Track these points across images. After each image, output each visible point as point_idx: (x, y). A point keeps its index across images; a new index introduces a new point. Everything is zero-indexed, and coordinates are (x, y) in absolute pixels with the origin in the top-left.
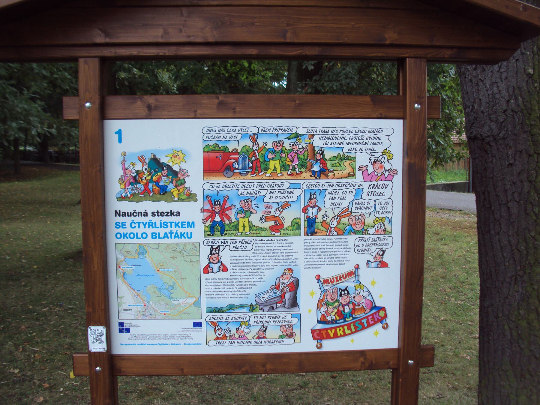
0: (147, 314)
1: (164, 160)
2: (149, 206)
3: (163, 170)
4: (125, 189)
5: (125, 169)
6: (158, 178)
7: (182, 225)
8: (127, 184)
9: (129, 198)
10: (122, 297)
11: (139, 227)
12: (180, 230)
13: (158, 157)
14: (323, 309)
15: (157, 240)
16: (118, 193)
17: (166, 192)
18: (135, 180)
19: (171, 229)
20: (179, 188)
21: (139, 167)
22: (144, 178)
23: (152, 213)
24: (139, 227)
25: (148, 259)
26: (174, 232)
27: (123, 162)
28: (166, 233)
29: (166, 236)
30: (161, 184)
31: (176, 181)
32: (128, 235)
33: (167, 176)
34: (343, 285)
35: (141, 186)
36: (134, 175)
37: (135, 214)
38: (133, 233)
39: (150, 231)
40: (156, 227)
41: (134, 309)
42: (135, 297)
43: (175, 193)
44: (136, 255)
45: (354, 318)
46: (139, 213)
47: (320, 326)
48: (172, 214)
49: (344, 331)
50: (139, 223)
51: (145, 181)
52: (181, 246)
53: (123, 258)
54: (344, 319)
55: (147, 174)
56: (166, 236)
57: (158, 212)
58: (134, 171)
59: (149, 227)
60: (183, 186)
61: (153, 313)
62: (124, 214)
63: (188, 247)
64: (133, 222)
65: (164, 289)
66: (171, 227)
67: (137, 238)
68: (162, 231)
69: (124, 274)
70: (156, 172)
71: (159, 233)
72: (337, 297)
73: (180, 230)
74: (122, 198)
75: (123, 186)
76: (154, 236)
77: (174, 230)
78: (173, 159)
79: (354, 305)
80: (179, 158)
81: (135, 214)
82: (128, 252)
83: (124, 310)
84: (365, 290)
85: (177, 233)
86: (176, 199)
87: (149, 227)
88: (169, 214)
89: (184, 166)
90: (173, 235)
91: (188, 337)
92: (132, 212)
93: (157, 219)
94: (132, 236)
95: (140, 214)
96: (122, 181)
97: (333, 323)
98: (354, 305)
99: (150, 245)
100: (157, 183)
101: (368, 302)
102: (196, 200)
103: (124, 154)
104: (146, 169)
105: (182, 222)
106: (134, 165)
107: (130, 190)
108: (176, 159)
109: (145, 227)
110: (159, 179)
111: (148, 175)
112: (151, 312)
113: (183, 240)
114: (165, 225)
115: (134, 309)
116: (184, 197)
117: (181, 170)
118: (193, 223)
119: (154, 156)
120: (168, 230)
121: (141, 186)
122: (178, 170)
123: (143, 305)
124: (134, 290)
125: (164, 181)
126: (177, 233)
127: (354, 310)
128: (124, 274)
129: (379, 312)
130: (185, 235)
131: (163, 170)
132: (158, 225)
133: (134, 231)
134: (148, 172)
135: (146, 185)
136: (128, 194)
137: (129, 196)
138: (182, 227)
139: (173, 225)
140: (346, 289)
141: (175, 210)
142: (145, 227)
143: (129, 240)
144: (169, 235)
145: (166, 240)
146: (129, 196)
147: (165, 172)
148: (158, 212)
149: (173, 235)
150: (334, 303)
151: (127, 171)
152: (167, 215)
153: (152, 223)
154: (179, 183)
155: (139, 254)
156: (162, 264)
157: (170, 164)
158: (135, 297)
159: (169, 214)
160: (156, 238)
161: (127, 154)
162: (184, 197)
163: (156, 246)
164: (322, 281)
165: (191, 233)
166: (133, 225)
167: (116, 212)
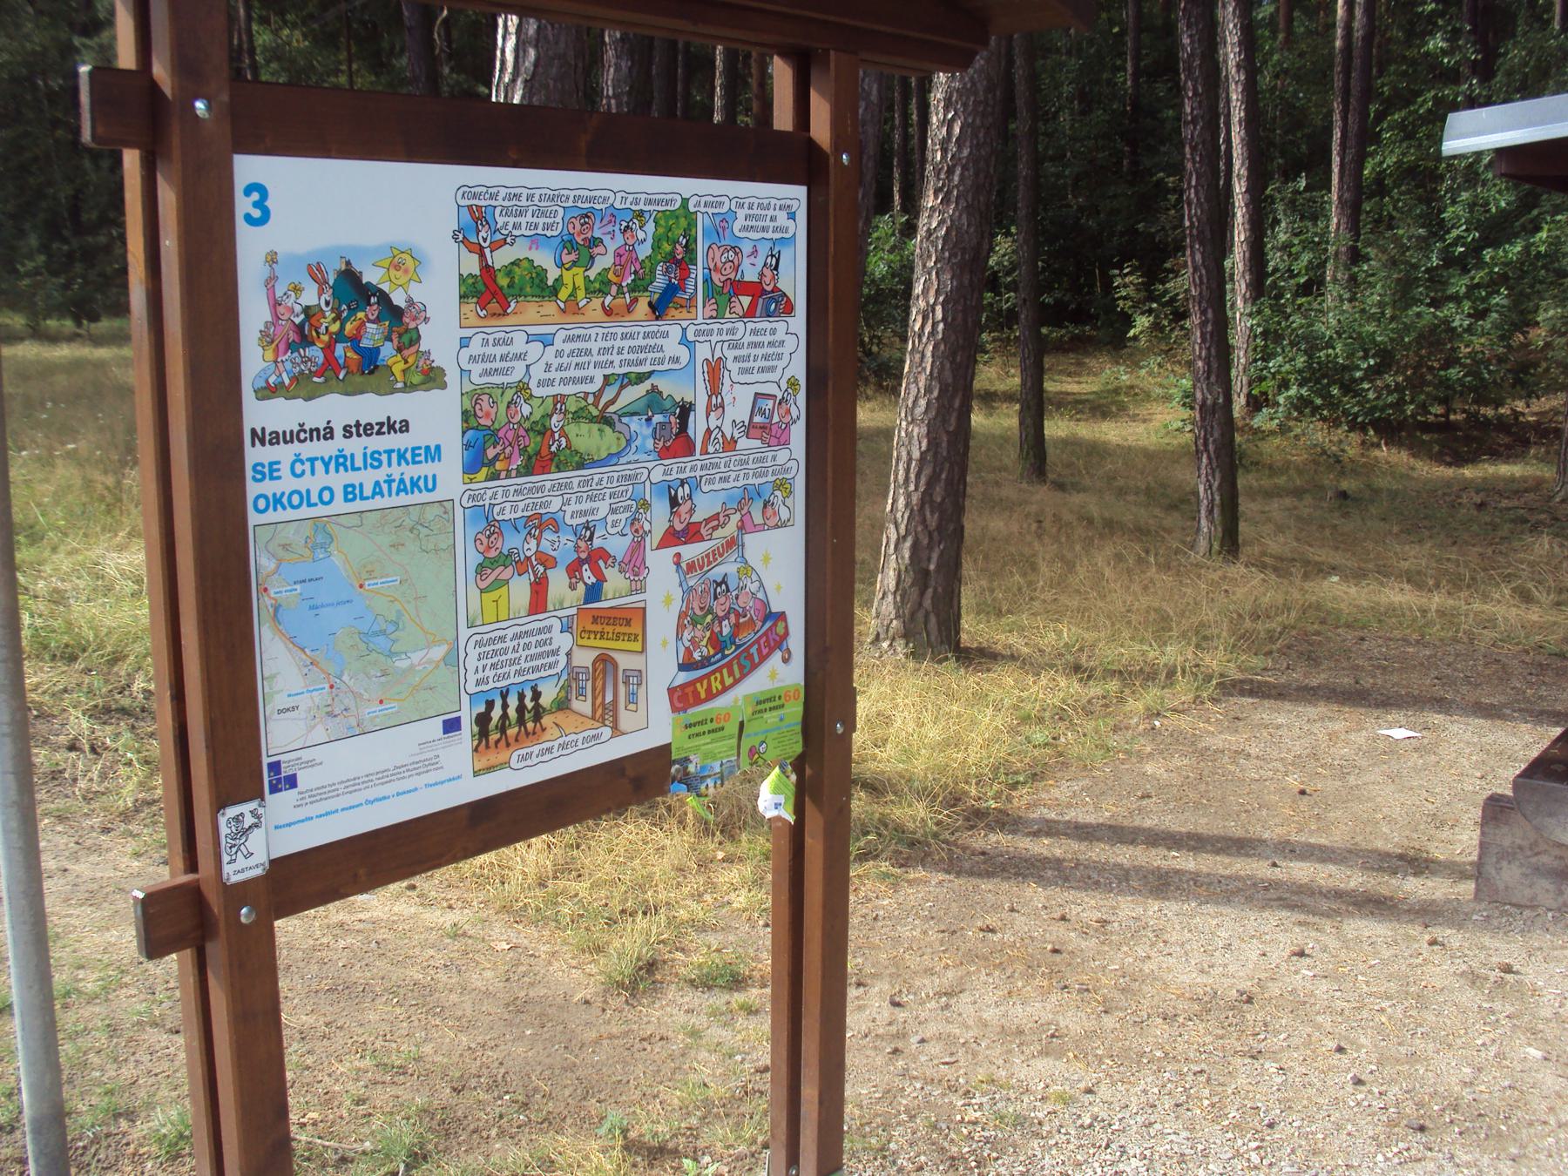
0: (337, 711)
1: (371, 276)
2: (336, 408)
3: (369, 304)
4: (276, 362)
5: (275, 304)
6: (358, 330)
7: (414, 455)
8: (282, 347)
9: (287, 388)
10: (273, 677)
11: (313, 473)
12: (410, 471)
13: (357, 267)
14: (687, 635)
15: (358, 505)
16: (258, 376)
17: (376, 367)
18: (303, 337)
19: (389, 471)
20: (406, 353)
21: (310, 296)
22: (322, 330)
23: (345, 429)
24: (313, 473)
25: (337, 559)
26: (397, 477)
27: (270, 283)
28: (377, 483)
29: (377, 490)
30: (365, 343)
31: (400, 335)
32: (285, 500)
33: (377, 321)
34: (717, 573)
35: (316, 353)
36: (297, 321)
37: (302, 436)
38: (299, 492)
39: (338, 480)
40: (354, 469)
41: (304, 702)
42: (305, 670)
43: (398, 369)
44: (307, 552)
45: (738, 647)
46: (311, 431)
47: (683, 677)
48: (391, 427)
49: (722, 682)
50: (312, 460)
51: (325, 338)
52: (415, 512)
53: (272, 565)
54: (721, 650)
55: (330, 315)
56: (377, 490)
57: (358, 425)
58: (298, 309)
59: (337, 471)
60: (413, 349)
61: (352, 705)
62: (276, 439)
63: (431, 513)
64: (298, 459)
65: (376, 634)
66: (390, 464)
67: (309, 505)
68: (368, 478)
69: (277, 608)
70: (352, 311)
71: (361, 485)
72: (709, 600)
73: (410, 471)
74: (269, 391)
75: (270, 355)
76: (351, 493)
77: (396, 471)
78: (393, 272)
79: (738, 615)
80: (406, 271)
81: (302, 436)
82: (285, 547)
83: (280, 712)
84: (754, 577)
85: (402, 481)
86: (400, 385)
87: (337, 471)
88: (385, 429)
89: (417, 293)
90: (394, 486)
91: (432, 764)
92: (296, 429)
93: (355, 446)
94: (296, 499)
95: (314, 434)
96: (267, 338)
97: (704, 667)
98: (738, 615)
99: (342, 520)
100: (355, 340)
101: (759, 606)
102: (444, 386)
103: (272, 259)
104: (327, 303)
105: (414, 449)
106: (297, 289)
107: (288, 365)
108: (399, 274)
109: (327, 472)
110: (359, 329)
111: (334, 320)
112: (346, 701)
113: (417, 498)
114: (373, 459)
115: (304, 702)
116: (417, 379)
117: (410, 302)
118: (438, 447)
119: (348, 263)
120: (381, 474)
121: (316, 353)
122: (403, 305)
123: (327, 686)
124: (303, 650)
125: (373, 334)
126: (402, 481)
127: (737, 628)
128: (277, 608)
129: (775, 625)
130: (421, 483)
131: (369, 304)
132: (359, 462)
133: (301, 484)
134: (332, 310)
135: (329, 349)
136: (285, 375)
137: (287, 382)
138: (415, 463)
139: (394, 456)
140: (724, 582)
141: (397, 417)
142: (327, 472)
143: (290, 514)
144: (385, 487)
145: (379, 502)
146: (287, 382)
147: (373, 311)
148: (358, 425)
149: (394, 486)
150: (705, 616)
151: (281, 310)
152: (379, 433)
153: (345, 457)
154: (406, 339)
155: (313, 549)
156: (369, 568)
157: (385, 287)
158: (305, 670)
159: (385, 429)
160: (354, 499)
161: (279, 258)
162: (417, 379)
163: (355, 520)
164: (684, 565)
165: (434, 477)
166: (299, 468)
167: (254, 431)
